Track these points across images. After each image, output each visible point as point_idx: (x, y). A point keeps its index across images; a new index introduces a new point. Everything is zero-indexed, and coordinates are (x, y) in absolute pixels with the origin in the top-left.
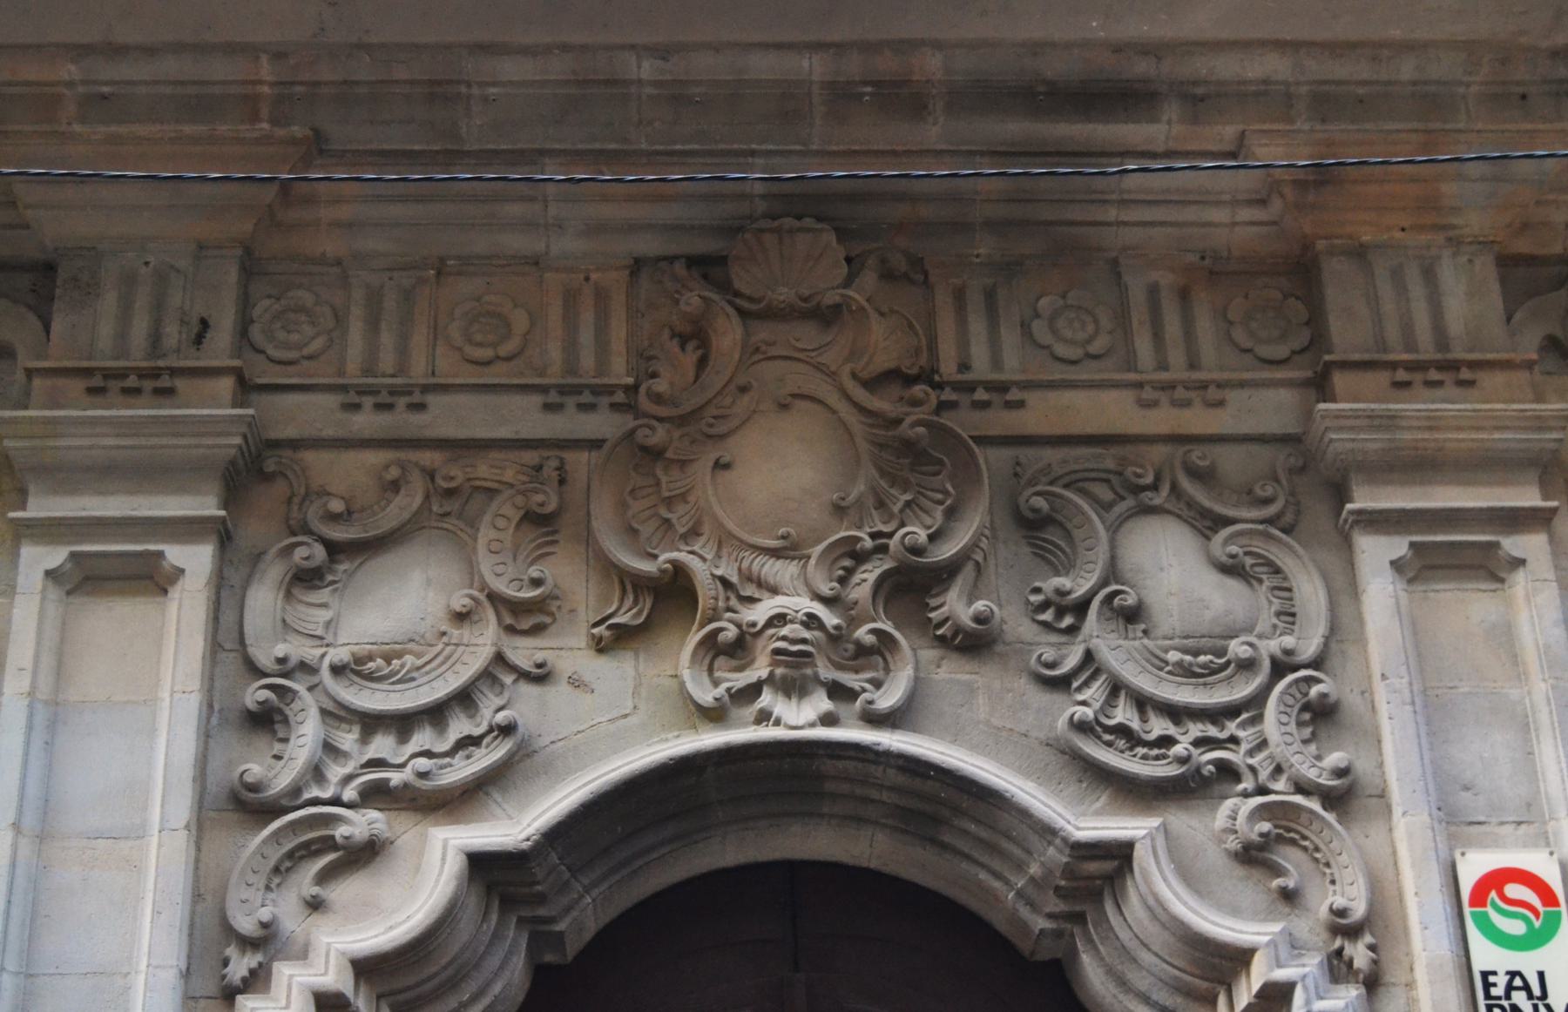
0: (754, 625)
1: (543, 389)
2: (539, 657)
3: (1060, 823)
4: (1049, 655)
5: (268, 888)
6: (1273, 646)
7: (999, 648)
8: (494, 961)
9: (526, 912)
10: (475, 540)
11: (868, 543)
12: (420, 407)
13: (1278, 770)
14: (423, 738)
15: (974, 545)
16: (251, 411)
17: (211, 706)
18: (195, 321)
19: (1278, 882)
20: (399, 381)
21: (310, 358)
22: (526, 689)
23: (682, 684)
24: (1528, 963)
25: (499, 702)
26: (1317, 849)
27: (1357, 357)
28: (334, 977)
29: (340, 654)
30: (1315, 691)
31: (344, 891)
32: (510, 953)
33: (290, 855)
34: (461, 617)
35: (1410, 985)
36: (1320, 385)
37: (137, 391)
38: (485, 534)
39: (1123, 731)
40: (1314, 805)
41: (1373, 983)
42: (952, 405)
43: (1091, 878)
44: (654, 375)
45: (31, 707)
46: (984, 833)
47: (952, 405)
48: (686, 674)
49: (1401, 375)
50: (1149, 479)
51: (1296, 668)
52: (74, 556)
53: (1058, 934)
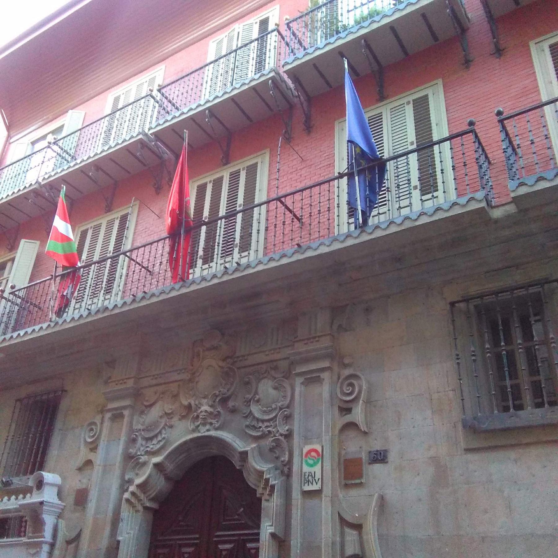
24: (312, 470)
39: (254, 426)
51: (283, 409)
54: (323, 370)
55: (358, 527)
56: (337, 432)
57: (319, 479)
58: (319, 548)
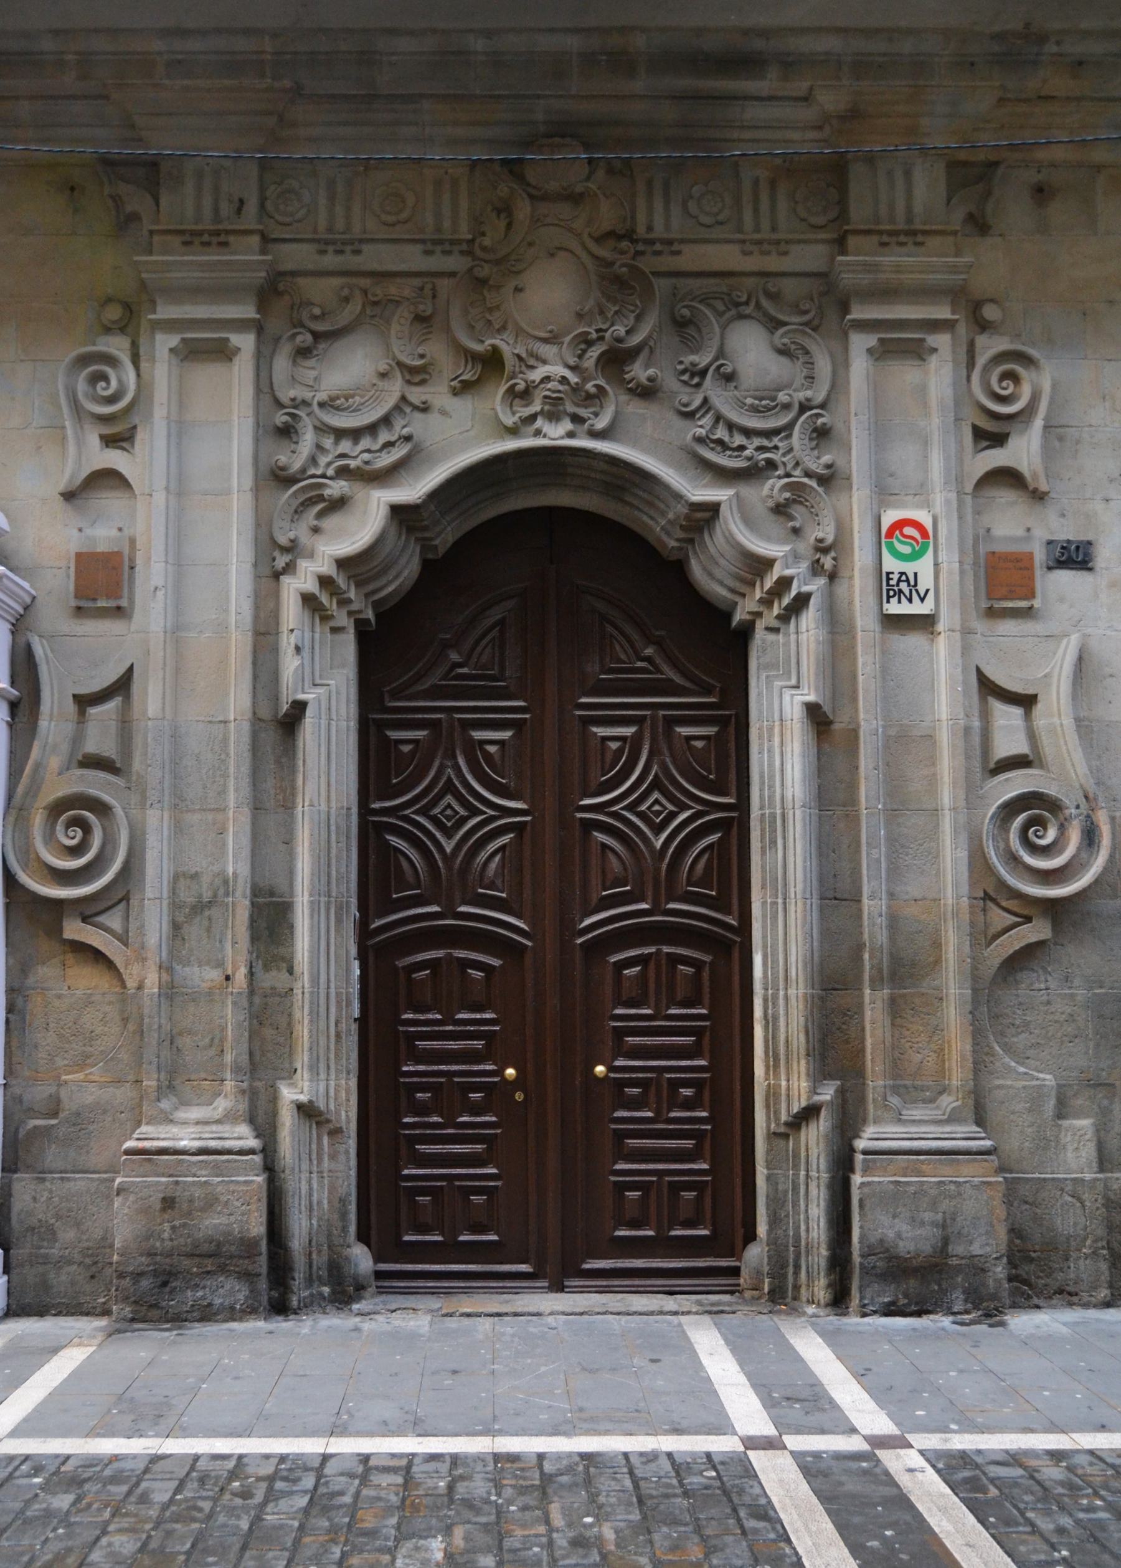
0: (534, 382)
1: (423, 241)
2: (423, 398)
3: (685, 492)
4: (685, 400)
5: (292, 521)
6: (801, 395)
7: (660, 395)
8: (403, 561)
9: (419, 535)
10: (389, 330)
11: (594, 335)
12: (357, 252)
13: (797, 464)
14: (365, 442)
15: (650, 337)
16: (269, 257)
17: (258, 424)
18: (236, 199)
19: (791, 524)
20: (348, 236)
21: (299, 221)
22: (418, 415)
23: (496, 414)
24: (909, 568)
25: (403, 423)
26: (812, 507)
27: (862, 227)
28: (327, 568)
29: (322, 396)
30: (820, 421)
31: (330, 523)
32: (412, 556)
33: (302, 504)
34: (383, 375)
35: (851, 578)
36: (840, 244)
37: (208, 244)
38: (395, 328)
39: (720, 442)
40: (813, 483)
41: (833, 577)
42: (642, 253)
43: (699, 520)
44: (483, 234)
45: (168, 424)
46: (645, 496)
47: (642, 253)
48: (499, 408)
49: (885, 239)
50: (744, 299)
51: (811, 409)
52: (183, 340)
53: (680, 549)
54: (935, 326)
55: (1026, 701)
56: (969, 487)
57: (927, 591)
58: (930, 738)
